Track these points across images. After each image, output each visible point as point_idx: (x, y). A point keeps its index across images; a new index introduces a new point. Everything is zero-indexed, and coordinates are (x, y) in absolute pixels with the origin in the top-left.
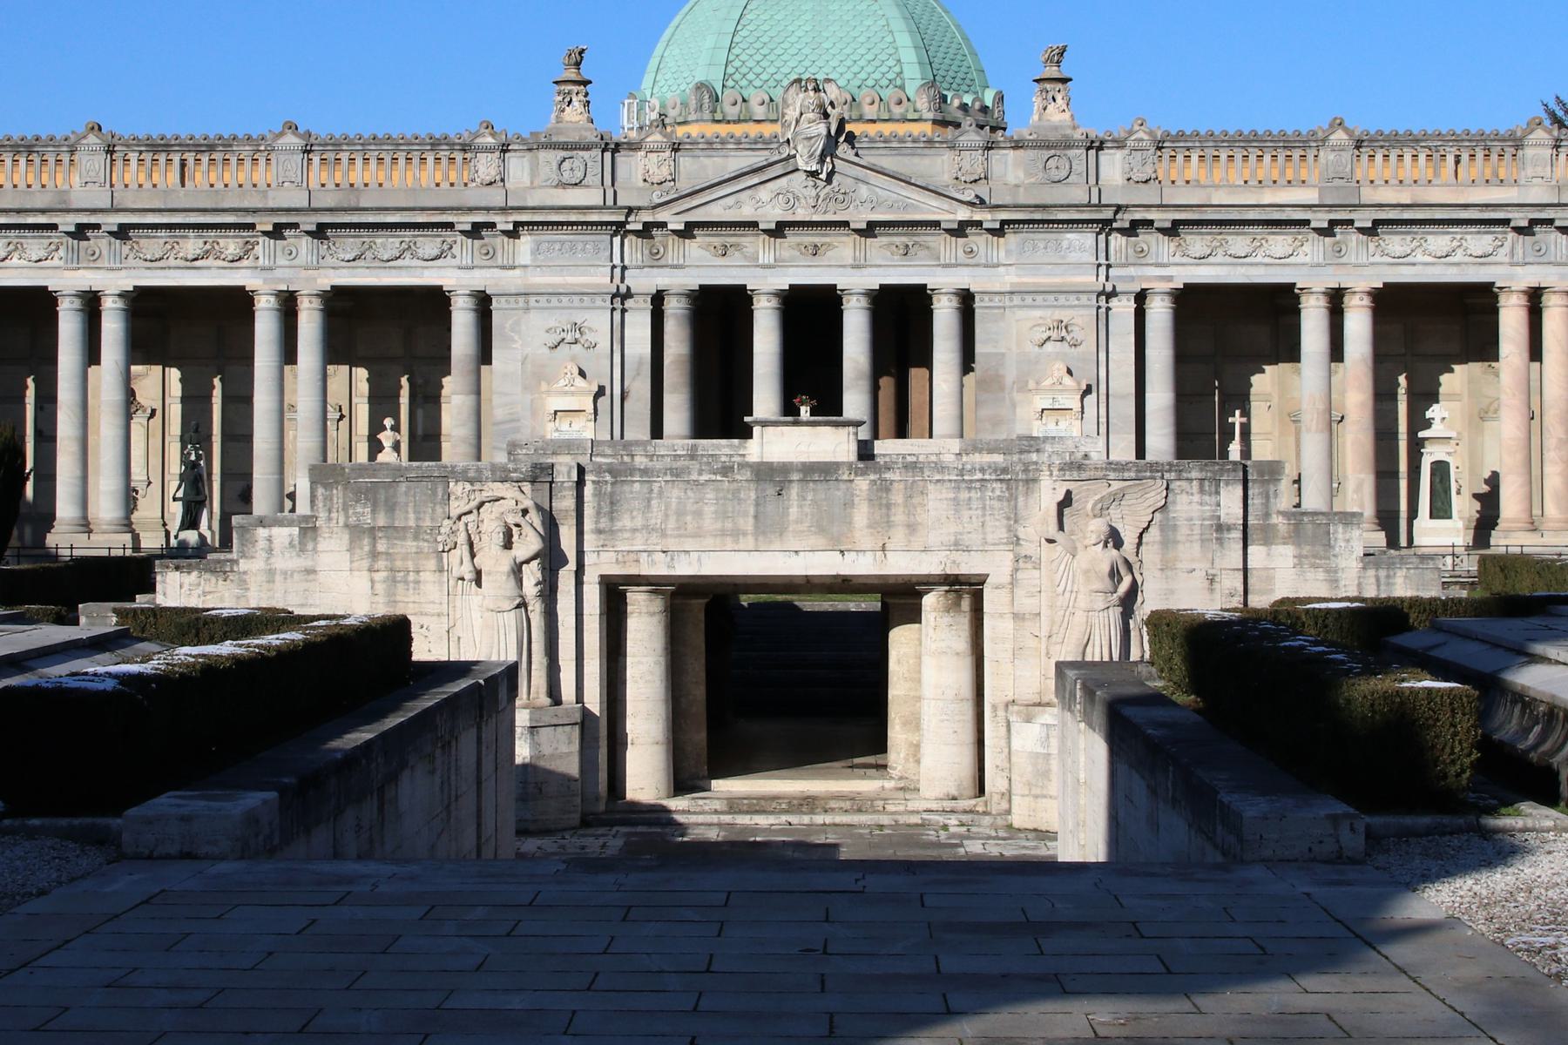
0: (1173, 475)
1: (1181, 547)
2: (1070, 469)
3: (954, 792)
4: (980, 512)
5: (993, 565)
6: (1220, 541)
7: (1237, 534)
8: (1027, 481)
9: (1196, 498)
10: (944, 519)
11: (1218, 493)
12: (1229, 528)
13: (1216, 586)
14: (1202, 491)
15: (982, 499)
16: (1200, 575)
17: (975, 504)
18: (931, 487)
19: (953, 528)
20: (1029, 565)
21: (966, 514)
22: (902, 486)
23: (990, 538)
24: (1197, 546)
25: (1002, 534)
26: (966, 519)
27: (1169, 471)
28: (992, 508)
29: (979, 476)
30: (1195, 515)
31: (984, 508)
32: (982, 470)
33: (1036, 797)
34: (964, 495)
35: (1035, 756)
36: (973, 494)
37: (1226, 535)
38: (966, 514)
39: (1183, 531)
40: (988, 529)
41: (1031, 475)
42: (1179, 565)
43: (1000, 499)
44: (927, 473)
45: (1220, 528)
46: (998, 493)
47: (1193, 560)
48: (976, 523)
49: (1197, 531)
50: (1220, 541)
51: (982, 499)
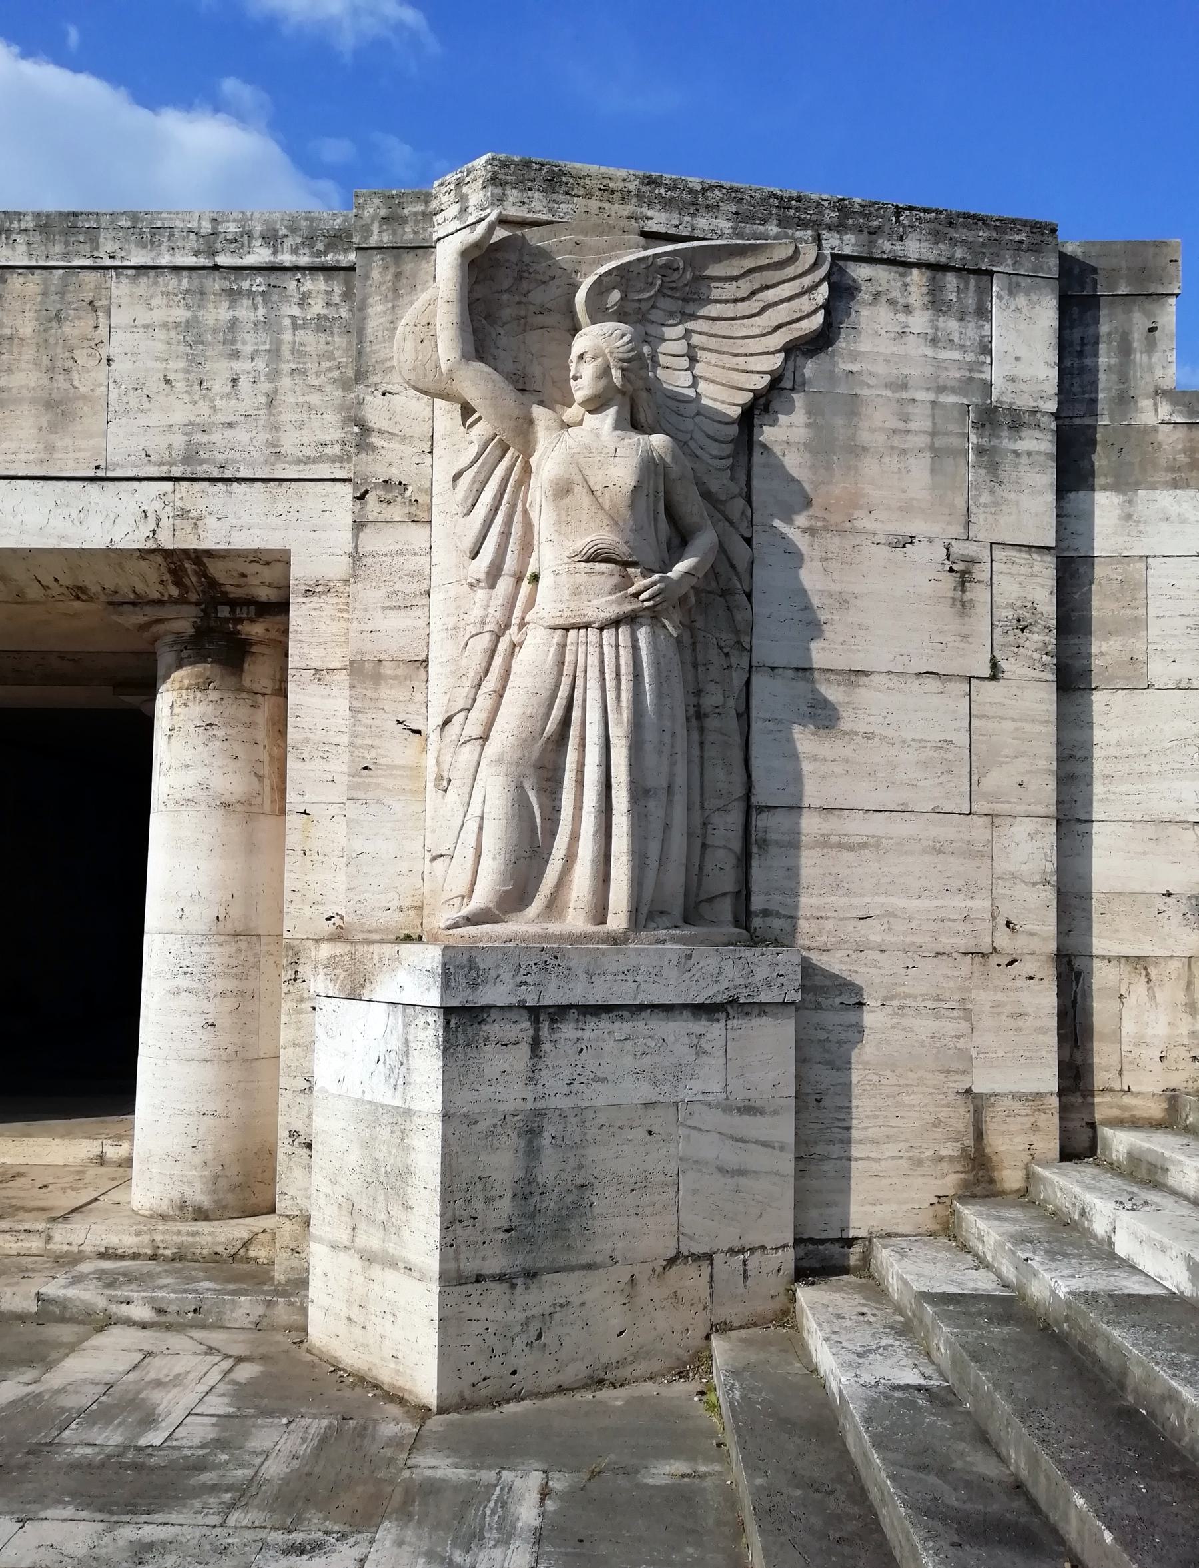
0: (849, 244)
1: (870, 467)
2: (522, 184)
3: (199, 1195)
4: (261, 364)
5: (307, 531)
6: (989, 458)
7: (1039, 444)
8: (397, 250)
9: (919, 321)
10: (154, 384)
11: (983, 313)
12: (1017, 421)
13: (979, 594)
14: (936, 303)
15: (270, 325)
16: (927, 555)
17: (248, 342)
18: (121, 288)
19: (181, 411)
20: (397, 512)
21: (219, 369)
22: (32, 285)
23: (290, 441)
24: (919, 470)
25: (329, 429)
26: (220, 386)
27: (840, 227)
28: (299, 352)
29: (261, 255)
30: (914, 371)
31: (275, 353)
32: (272, 239)
33: (369, 1258)
34: (217, 313)
35: (371, 1113)
36: (244, 312)
37: (1007, 443)
38: (219, 369)
39: (878, 417)
40: (288, 416)
41: (408, 235)
42: (866, 523)
43: (323, 325)
44: (107, 245)
45: (993, 418)
46: (317, 307)
47: (907, 509)
48: (250, 397)
49: (920, 422)
50: (989, 458)
51: (270, 325)
